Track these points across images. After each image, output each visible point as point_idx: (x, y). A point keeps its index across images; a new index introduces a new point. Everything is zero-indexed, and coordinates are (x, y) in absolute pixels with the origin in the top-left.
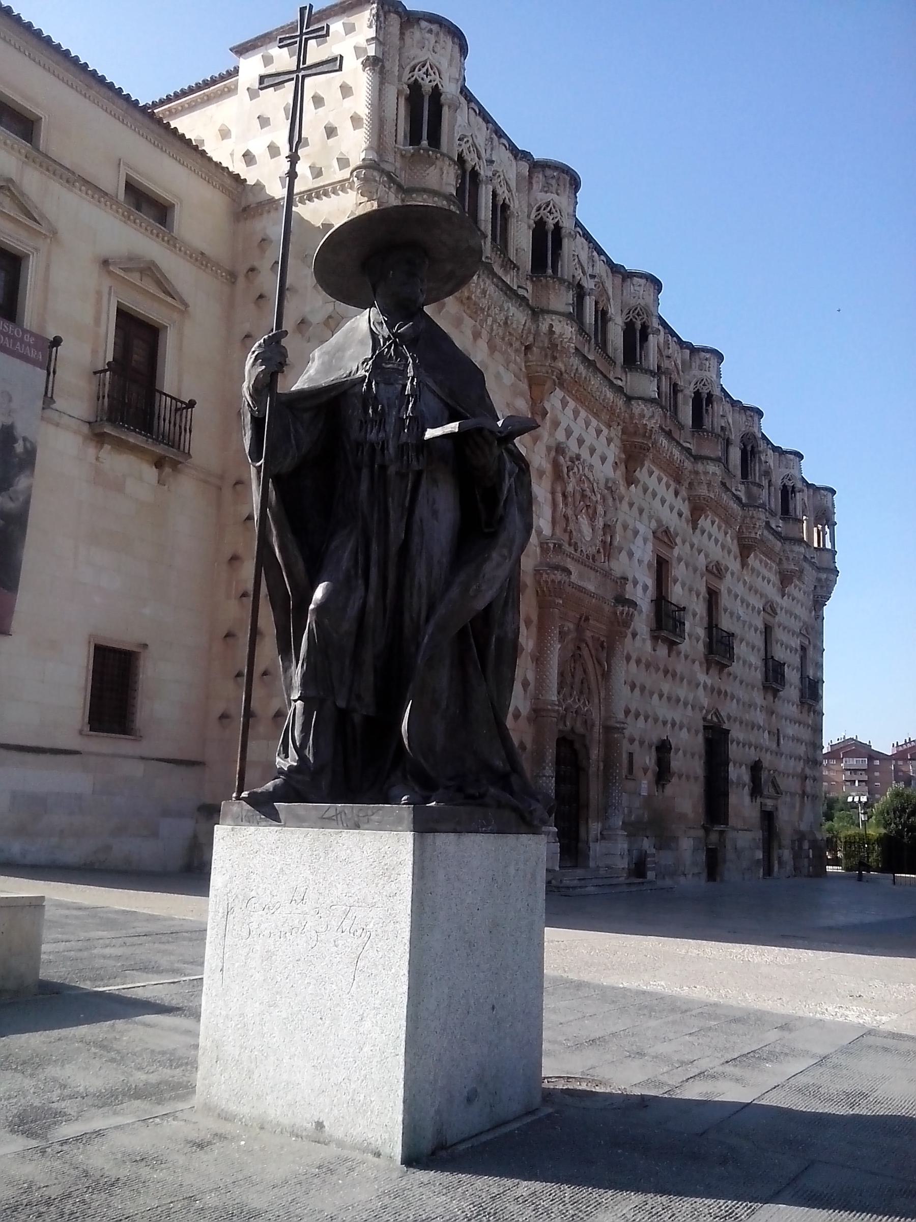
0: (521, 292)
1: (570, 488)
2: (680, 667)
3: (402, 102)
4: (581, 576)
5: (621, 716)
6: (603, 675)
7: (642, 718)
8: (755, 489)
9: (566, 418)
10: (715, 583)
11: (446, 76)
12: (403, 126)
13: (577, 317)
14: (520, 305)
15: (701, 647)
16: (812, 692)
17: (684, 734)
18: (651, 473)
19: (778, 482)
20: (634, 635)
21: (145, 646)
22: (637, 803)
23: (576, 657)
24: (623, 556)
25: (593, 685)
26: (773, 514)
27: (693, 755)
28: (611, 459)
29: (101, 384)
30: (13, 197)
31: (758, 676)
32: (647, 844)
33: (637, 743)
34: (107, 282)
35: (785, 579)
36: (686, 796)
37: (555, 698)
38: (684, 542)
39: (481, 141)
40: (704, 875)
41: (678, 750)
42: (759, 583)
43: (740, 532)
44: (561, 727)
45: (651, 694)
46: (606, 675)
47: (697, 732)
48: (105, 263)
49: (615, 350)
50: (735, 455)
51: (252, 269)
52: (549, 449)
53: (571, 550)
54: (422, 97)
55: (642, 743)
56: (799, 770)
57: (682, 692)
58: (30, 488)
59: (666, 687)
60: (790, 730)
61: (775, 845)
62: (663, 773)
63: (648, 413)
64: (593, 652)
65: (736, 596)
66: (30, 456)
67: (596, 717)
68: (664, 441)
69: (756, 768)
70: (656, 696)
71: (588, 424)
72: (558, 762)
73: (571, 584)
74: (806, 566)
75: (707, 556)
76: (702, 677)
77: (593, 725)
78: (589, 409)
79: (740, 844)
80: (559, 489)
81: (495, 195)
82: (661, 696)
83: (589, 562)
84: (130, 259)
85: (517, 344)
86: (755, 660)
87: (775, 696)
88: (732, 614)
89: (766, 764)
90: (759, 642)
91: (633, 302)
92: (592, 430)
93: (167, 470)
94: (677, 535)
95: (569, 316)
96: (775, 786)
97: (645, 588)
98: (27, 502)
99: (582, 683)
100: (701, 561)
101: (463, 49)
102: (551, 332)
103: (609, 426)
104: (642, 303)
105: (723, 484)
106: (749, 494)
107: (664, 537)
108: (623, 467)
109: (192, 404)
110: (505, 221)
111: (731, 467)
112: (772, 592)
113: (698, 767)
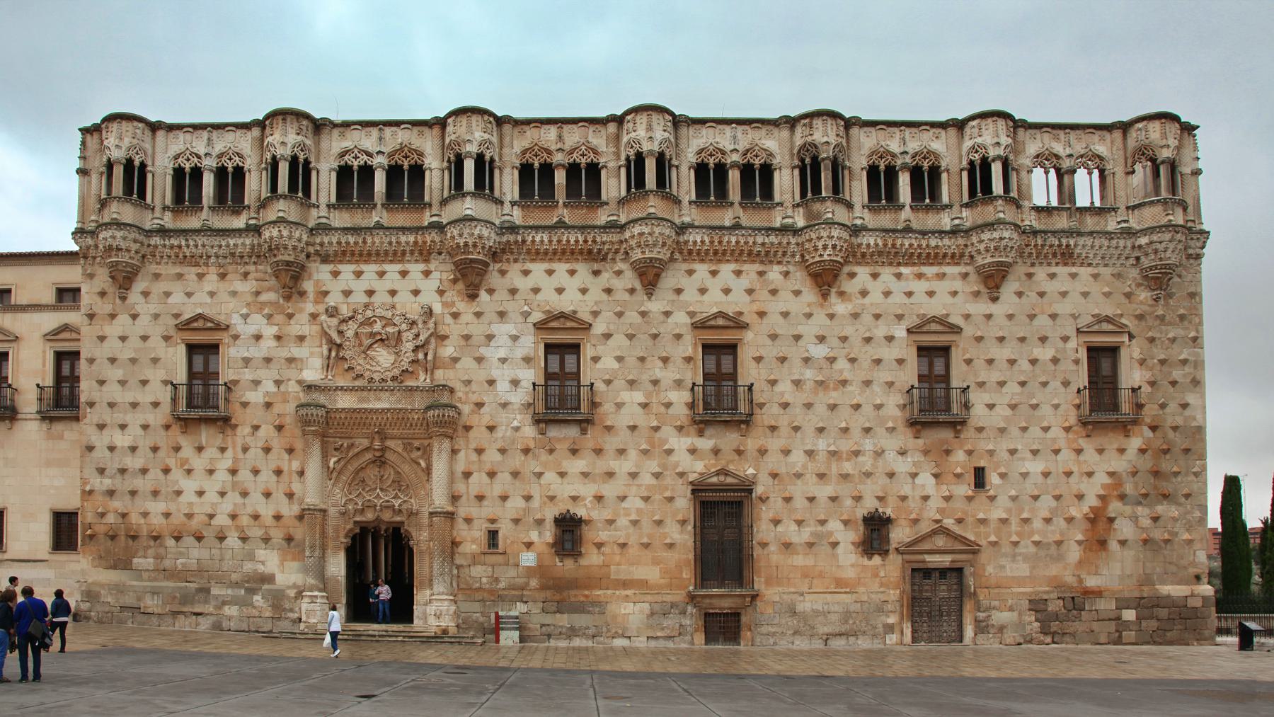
17: (634, 503)
20: (491, 429)
24: (467, 363)
45: (540, 475)
46: (428, 471)
59: (577, 465)
75: (691, 314)
76: (681, 443)
85: (254, 259)
94: (595, 314)
97: (515, 383)
103: (427, 261)
108: (460, 285)
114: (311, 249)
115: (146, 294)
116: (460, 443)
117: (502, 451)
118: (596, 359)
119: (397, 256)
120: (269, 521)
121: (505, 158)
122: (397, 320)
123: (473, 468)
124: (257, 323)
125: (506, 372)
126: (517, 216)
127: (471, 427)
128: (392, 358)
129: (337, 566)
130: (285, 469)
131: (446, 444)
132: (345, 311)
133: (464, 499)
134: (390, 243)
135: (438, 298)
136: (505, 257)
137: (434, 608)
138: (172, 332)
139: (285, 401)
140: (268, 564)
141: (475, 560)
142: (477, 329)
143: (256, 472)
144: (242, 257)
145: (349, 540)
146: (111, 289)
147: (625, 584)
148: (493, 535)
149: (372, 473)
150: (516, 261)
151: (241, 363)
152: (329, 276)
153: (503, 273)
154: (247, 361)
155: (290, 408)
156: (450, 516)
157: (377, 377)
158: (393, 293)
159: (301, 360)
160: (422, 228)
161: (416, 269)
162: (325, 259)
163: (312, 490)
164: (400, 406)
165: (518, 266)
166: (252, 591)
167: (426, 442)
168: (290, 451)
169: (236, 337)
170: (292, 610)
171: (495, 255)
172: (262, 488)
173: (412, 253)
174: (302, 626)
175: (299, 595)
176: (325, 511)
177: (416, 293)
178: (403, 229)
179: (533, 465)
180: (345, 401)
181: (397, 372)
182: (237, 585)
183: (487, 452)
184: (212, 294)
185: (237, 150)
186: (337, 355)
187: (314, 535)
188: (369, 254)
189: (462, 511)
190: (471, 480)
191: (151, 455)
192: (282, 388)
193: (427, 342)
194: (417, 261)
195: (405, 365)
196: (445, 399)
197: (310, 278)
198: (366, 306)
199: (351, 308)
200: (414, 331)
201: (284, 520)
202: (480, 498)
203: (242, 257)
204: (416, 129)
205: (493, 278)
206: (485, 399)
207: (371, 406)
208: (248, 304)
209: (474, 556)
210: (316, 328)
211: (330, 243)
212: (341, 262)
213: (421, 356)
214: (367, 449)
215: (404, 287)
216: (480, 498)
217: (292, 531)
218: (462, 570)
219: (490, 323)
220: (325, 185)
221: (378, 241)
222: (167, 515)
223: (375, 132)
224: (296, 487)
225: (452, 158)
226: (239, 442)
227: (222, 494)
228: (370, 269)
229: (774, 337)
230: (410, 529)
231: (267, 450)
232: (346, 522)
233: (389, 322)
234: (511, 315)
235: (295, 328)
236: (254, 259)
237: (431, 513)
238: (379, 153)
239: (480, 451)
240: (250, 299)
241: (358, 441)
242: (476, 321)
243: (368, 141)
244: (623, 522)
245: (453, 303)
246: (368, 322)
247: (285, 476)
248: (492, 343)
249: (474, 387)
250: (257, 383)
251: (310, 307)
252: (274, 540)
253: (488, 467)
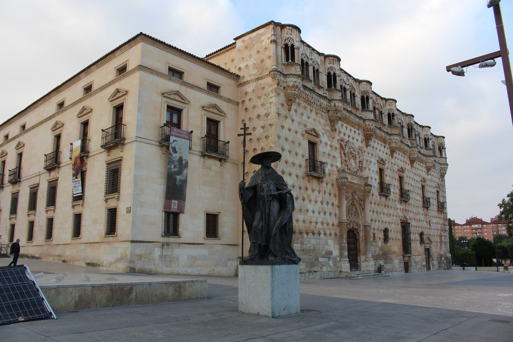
0: (325, 95)
1: (346, 151)
2: (391, 203)
3: (283, 50)
4: (352, 179)
5: (369, 222)
7: (377, 222)
8: (413, 142)
9: (343, 130)
10: (401, 174)
11: (295, 41)
12: (284, 56)
13: (344, 100)
15: (398, 196)
16: (442, 207)
17: (393, 225)
18: (375, 142)
19: (423, 137)
20: (373, 195)
21: (220, 213)
22: (377, 249)
23: (353, 204)
24: (367, 170)
25: (359, 213)
26: (421, 148)
27: (397, 232)
28: (360, 140)
29: (204, 141)
30: (179, 95)
31: (421, 203)
32: (381, 262)
33: (376, 230)
34: (204, 112)
35: (428, 169)
36: (395, 245)
37: (345, 218)
38: (389, 162)
39: (308, 54)
40: (404, 271)
41: (391, 231)
42: (418, 172)
43: (409, 156)
44: (349, 227)
45: (380, 213)
46: (363, 209)
47: (398, 224)
48: (203, 107)
49: (358, 105)
50: (405, 131)
51: (243, 101)
52: (338, 140)
53: (348, 171)
54: (288, 48)
55: (378, 230)
56: (439, 234)
57: (392, 212)
58: (187, 173)
59: (386, 211)
60: (434, 220)
61: (431, 259)
62: (386, 239)
63: (371, 124)
65: (410, 178)
66: (187, 163)
67: (361, 223)
68: (378, 131)
69: (421, 235)
70: (382, 214)
71: (351, 130)
72: (348, 237)
73: (349, 182)
74: (436, 164)
75: (398, 166)
76: (399, 206)
77: (360, 225)
78: (351, 125)
79: (417, 260)
80: (342, 153)
81: (314, 68)
82: (384, 214)
83: (354, 174)
84: (210, 105)
85: (325, 111)
86: (419, 198)
87: (427, 209)
88: (409, 184)
89: (425, 233)
90: (420, 192)
91: (363, 90)
92: (353, 132)
93: (223, 161)
95: (340, 100)
96: (429, 239)
97: (376, 179)
98: (187, 177)
100: (396, 168)
101: (299, 31)
102: (335, 106)
104: (366, 90)
105: (402, 142)
106: (412, 143)
107: (381, 162)
108: (364, 142)
109: (228, 142)
110: (318, 74)
111: (404, 135)
112: (424, 174)
113: (400, 236)
115: (296, 111)
118: (386, 176)
120: (331, 226)
138: (304, 133)
146: (285, 105)
147: (394, 253)
166: (329, 258)
168: (335, 196)
179: (379, 209)
182: (323, 257)
184: (315, 120)
191: (299, 191)
222: (304, 222)
225: (365, 97)
226: (323, 190)
227: (319, 213)
229: (407, 176)
237: (365, 226)
244: (392, 232)
251: (337, 137)
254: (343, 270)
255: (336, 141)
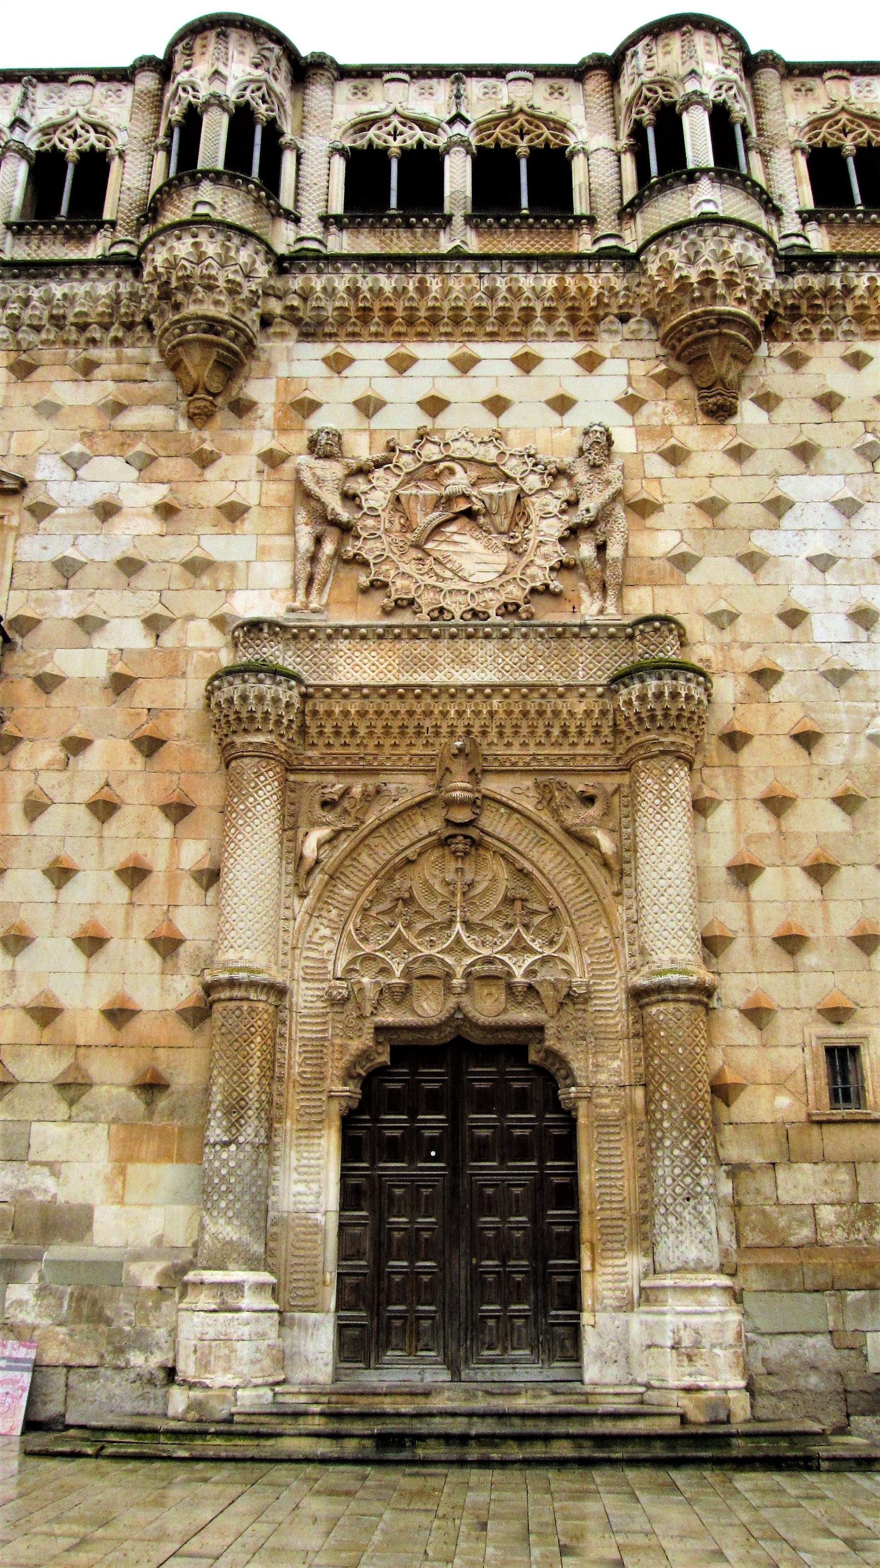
6: (606, 865)
14: (84, 274)
63: (675, 255)
64: (545, 817)
80: (302, 516)
85: (116, 331)
99: (509, 901)
103: (587, 335)
108: (684, 389)
114: (275, 307)
116: (718, 783)
117: (847, 802)
119: (509, 322)
121: (770, 131)
122: (512, 467)
123: (761, 854)
124: (110, 476)
125: (836, 593)
126: (819, 240)
127: (746, 738)
128: (503, 558)
129: (311, 1180)
130: (159, 863)
131: (680, 783)
132: (361, 449)
133: (738, 949)
134: (492, 293)
135: (625, 417)
136: (798, 328)
137: (660, 1326)
139: (175, 672)
140: (72, 1172)
141: (788, 1146)
142: (741, 489)
143: (61, 874)
144: (83, 328)
145: (353, 1088)
148: (842, 1060)
149: (434, 874)
150: (826, 336)
151: (50, 576)
152: (322, 369)
153: (795, 361)
154: (67, 569)
155: (191, 691)
156: (702, 995)
157: (456, 606)
158: (497, 405)
159: (232, 567)
160: (579, 257)
161: (559, 355)
162: (311, 332)
163: (254, 921)
164: (529, 679)
165: (835, 349)
167: (610, 782)
168: (178, 811)
169: (41, 511)
170: (141, 1341)
171: (773, 322)
172: (75, 921)
173: (550, 315)
174: (179, 1400)
175: (176, 1281)
176: (280, 991)
177: (562, 404)
178: (527, 260)
180: (359, 667)
181: (516, 593)
183: (802, 806)
185: (95, 119)
186: (337, 555)
187: (241, 1070)
188: (434, 320)
189: (734, 990)
190: (760, 888)
192: (169, 639)
193: (604, 515)
194: (562, 335)
195: (539, 576)
196: (671, 652)
197: (266, 376)
198: (423, 436)
199: (381, 442)
200: (564, 490)
201: (138, 1026)
202: (791, 943)
203: (83, 328)
204: (542, 85)
205: (770, 367)
206: (781, 661)
207: (439, 678)
208: (88, 436)
209: (784, 1132)
210: (279, 489)
211: (330, 292)
212: (354, 336)
213: (586, 550)
214: (423, 804)
215: (528, 394)
216: (791, 943)
217: (164, 1060)
218: (749, 1183)
219: (776, 475)
220: (317, 180)
221: (458, 287)
223: (443, 88)
224: (191, 921)
228: (433, 357)
230: (565, 1049)
231: (104, 809)
232: (349, 1032)
233: (493, 471)
234: (829, 455)
235: (215, 488)
236: (116, 331)
237: (639, 996)
238: (451, 122)
239: (777, 804)
240: (92, 422)
241: (393, 783)
242: (731, 466)
243: (432, 102)
245: (668, 430)
246: (432, 472)
247: (155, 888)
248: (787, 521)
249: (744, 630)
250: (89, 625)
252: (100, 1092)
253: (808, 851)
254: (187, 1368)
255: (247, 464)
